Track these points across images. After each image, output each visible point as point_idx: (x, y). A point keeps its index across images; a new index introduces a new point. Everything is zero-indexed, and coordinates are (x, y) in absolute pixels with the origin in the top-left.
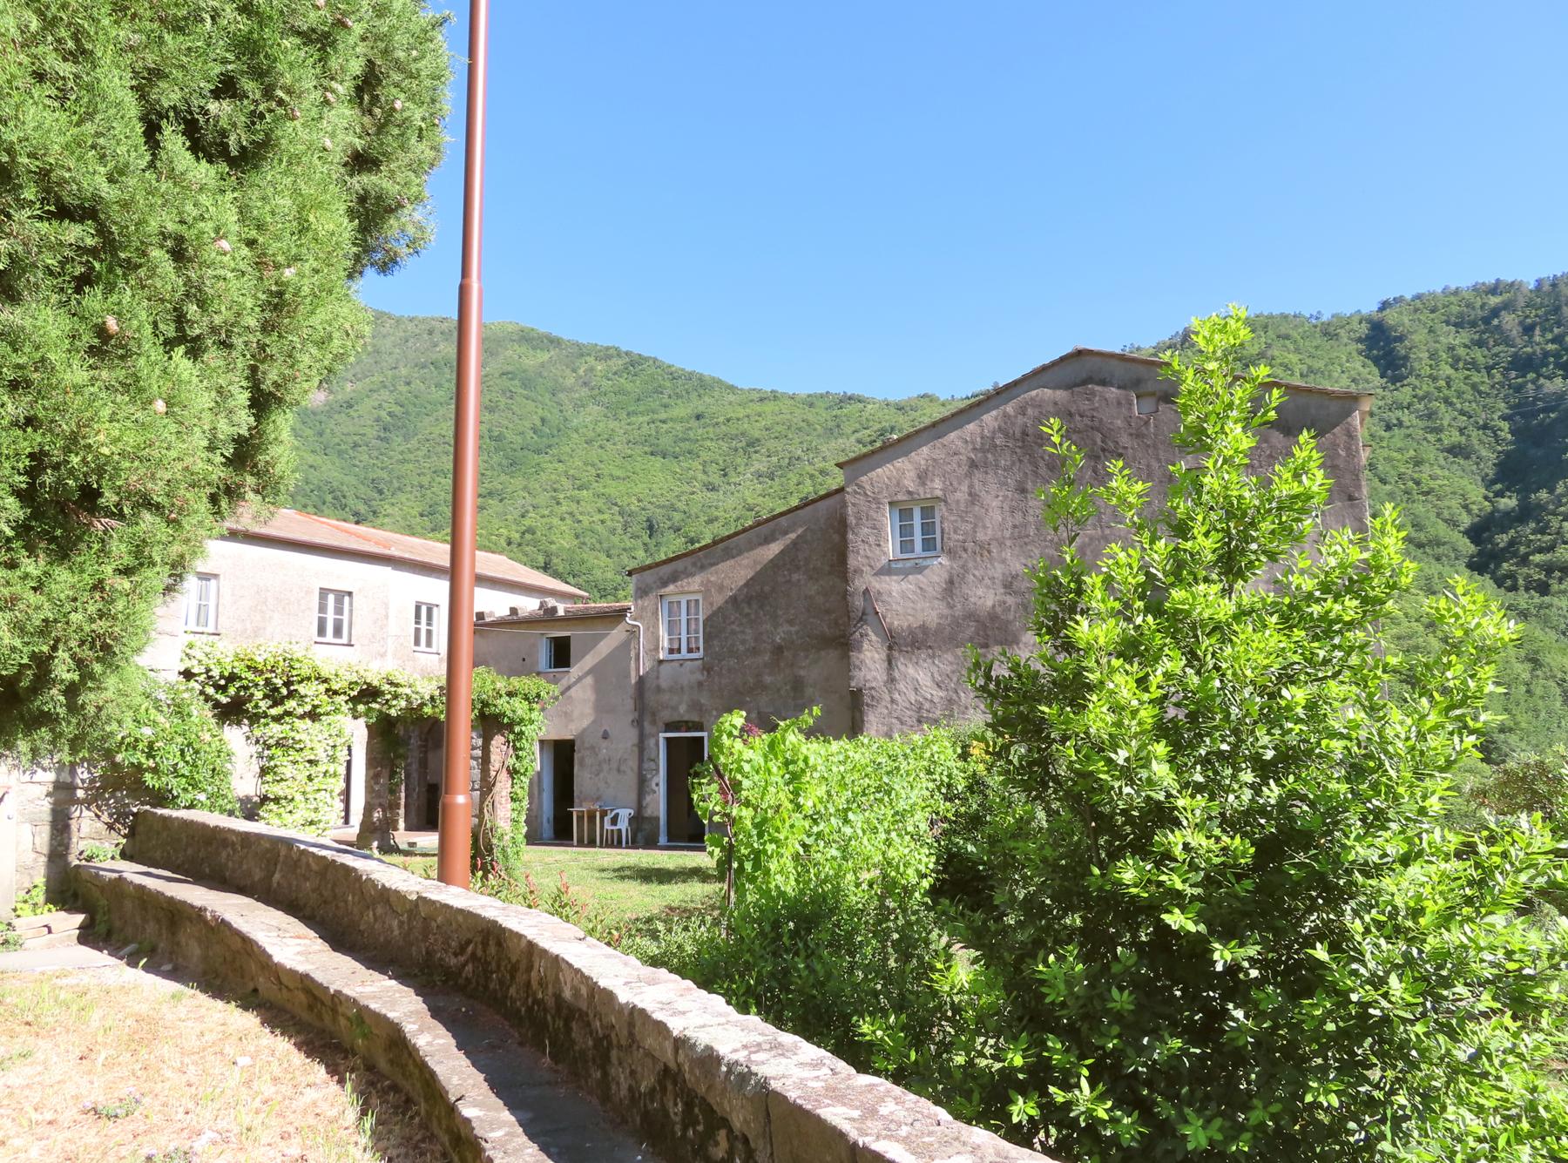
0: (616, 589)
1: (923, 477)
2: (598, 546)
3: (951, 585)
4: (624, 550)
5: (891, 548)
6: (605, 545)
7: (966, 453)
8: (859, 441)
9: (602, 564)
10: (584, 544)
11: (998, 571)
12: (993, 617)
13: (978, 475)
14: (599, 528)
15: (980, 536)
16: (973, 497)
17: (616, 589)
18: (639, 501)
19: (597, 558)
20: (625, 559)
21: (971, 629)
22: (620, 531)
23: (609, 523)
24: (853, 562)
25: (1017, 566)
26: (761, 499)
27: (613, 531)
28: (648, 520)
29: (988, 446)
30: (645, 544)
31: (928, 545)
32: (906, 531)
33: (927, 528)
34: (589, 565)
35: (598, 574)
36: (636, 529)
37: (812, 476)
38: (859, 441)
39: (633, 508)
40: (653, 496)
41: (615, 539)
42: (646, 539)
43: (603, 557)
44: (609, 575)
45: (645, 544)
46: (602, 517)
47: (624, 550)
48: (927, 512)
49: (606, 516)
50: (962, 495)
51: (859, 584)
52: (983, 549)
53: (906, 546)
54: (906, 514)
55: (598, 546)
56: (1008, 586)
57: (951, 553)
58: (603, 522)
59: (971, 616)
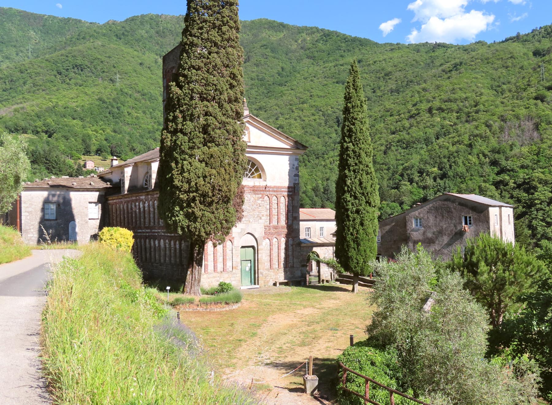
0: (323, 154)
1: (419, 214)
2: (313, 133)
3: (424, 233)
4: (326, 134)
5: (414, 226)
6: (317, 132)
7: (427, 210)
8: (443, 71)
9: (316, 142)
10: (307, 132)
11: (432, 231)
12: (431, 239)
13: (429, 214)
14: (313, 123)
15: (429, 225)
16: (428, 218)
17: (323, 154)
18: (332, 108)
19: (313, 139)
20: (326, 138)
21: (427, 241)
22: (323, 124)
23: (318, 120)
24: (408, 228)
25: (435, 230)
26: (393, 105)
27: (320, 124)
28: (337, 118)
29: (430, 209)
30: (336, 130)
31: (421, 225)
32: (417, 222)
33: (420, 222)
34: (310, 143)
35: (314, 147)
36: (331, 123)
37: (418, 92)
38: (443, 71)
39: (329, 112)
40: (339, 105)
41: (321, 129)
42: (336, 127)
43: (317, 138)
44: (320, 147)
45: (336, 130)
46: (313, 117)
47: (326, 134)
48: (420, 219)
49: (317, 117)
50: (426, 217)
51: (409, 232)
52: (429, 227)
53: (417, 225)
54: (417, 220)
55: (313, 133)
56: (434, 233)
57: (424, 227)
58: (315, 120)
59: (427, 238)
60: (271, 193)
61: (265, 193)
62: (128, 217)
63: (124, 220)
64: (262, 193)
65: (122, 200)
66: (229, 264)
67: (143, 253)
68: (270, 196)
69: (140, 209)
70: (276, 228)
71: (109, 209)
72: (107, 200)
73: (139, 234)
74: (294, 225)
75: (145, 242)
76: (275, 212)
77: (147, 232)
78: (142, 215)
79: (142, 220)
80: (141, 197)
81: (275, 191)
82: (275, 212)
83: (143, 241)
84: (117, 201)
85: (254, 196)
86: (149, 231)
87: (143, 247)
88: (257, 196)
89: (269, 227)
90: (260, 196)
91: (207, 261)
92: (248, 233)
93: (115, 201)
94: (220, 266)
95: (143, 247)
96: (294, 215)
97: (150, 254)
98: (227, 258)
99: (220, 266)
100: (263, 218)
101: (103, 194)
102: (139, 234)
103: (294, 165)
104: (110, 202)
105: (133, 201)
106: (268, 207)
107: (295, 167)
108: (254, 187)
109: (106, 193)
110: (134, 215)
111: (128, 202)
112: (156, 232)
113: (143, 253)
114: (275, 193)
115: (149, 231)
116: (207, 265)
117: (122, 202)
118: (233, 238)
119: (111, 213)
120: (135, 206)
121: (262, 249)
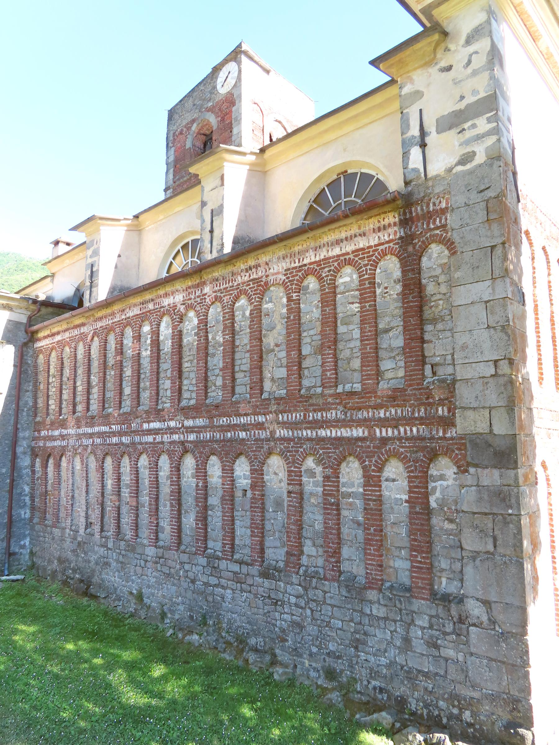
62: (104, 380)
63: (89, 393)
65: (84, 329)
67: (165, 510)
69: (156, 343)
71: (36, 366)
72: (32, 337)
75: (177, 469)
77: (190, 430)
78: (166, 366)
79: (166, 384)
80: (166, 302)
83: (164, 462)
84: (67, 335)
86: (200, 422)
87: (166, 489)
93: (58, 338)
95: (166, 489)
101: (24, 319)
105: (128, 323)
110: (128, 372)
111: (109, 329)
112: (244, 427)
113: (165, 510)
115: (200, 422)
117: (82, 338)
119: (42, 378)
120: (138, 337)
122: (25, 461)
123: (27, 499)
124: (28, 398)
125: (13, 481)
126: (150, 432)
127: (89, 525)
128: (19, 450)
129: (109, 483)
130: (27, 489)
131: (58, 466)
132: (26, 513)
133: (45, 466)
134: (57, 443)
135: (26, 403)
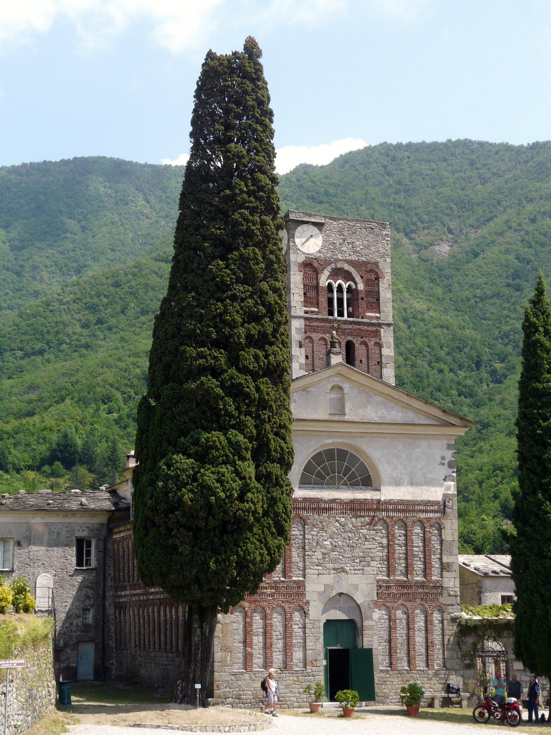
60: (391, 514)
61: (378, 513)
64: (372, 514)
66: (298, 655)
68: (388, 520)
70: (402, 585)
73: (151, 597)
74: (445, 580)
76: (400, 551)
81: (399, 511)
82: (400, 551)
85: (354, 520)
88: (358, 519)
89: (388, 582)
90: (367, 519)
91: (251, 647)
92: (341, 594)
93: (122, 535)
94: (277, 658)
95: (156, 622)
96: (445, 560)
97: (165, 636)
98: (294, 641)
99: (277, 658)
100: (373, 563)
102: (151, 597)
103: (443, 458)
104: (115, 537)
106: (385, 541)
107: (446, 462)
108: (352, 501)
109: (109, 520)
114: (401, 515)
116: (251, 655)
118: (308, 603)
121: (371, 628)
122: (110, 611)
123: (113, 635)
124: (111, 571)
125: (104, 623)
126: (152, 593)
127: (135, 647)
128: (107, 604)
129: (142, 621)
130: (113, 628)
131: (125, 613)
132: (112, 644)
133: (120, 614)
134: (123, 600)
135: (110, 574)
